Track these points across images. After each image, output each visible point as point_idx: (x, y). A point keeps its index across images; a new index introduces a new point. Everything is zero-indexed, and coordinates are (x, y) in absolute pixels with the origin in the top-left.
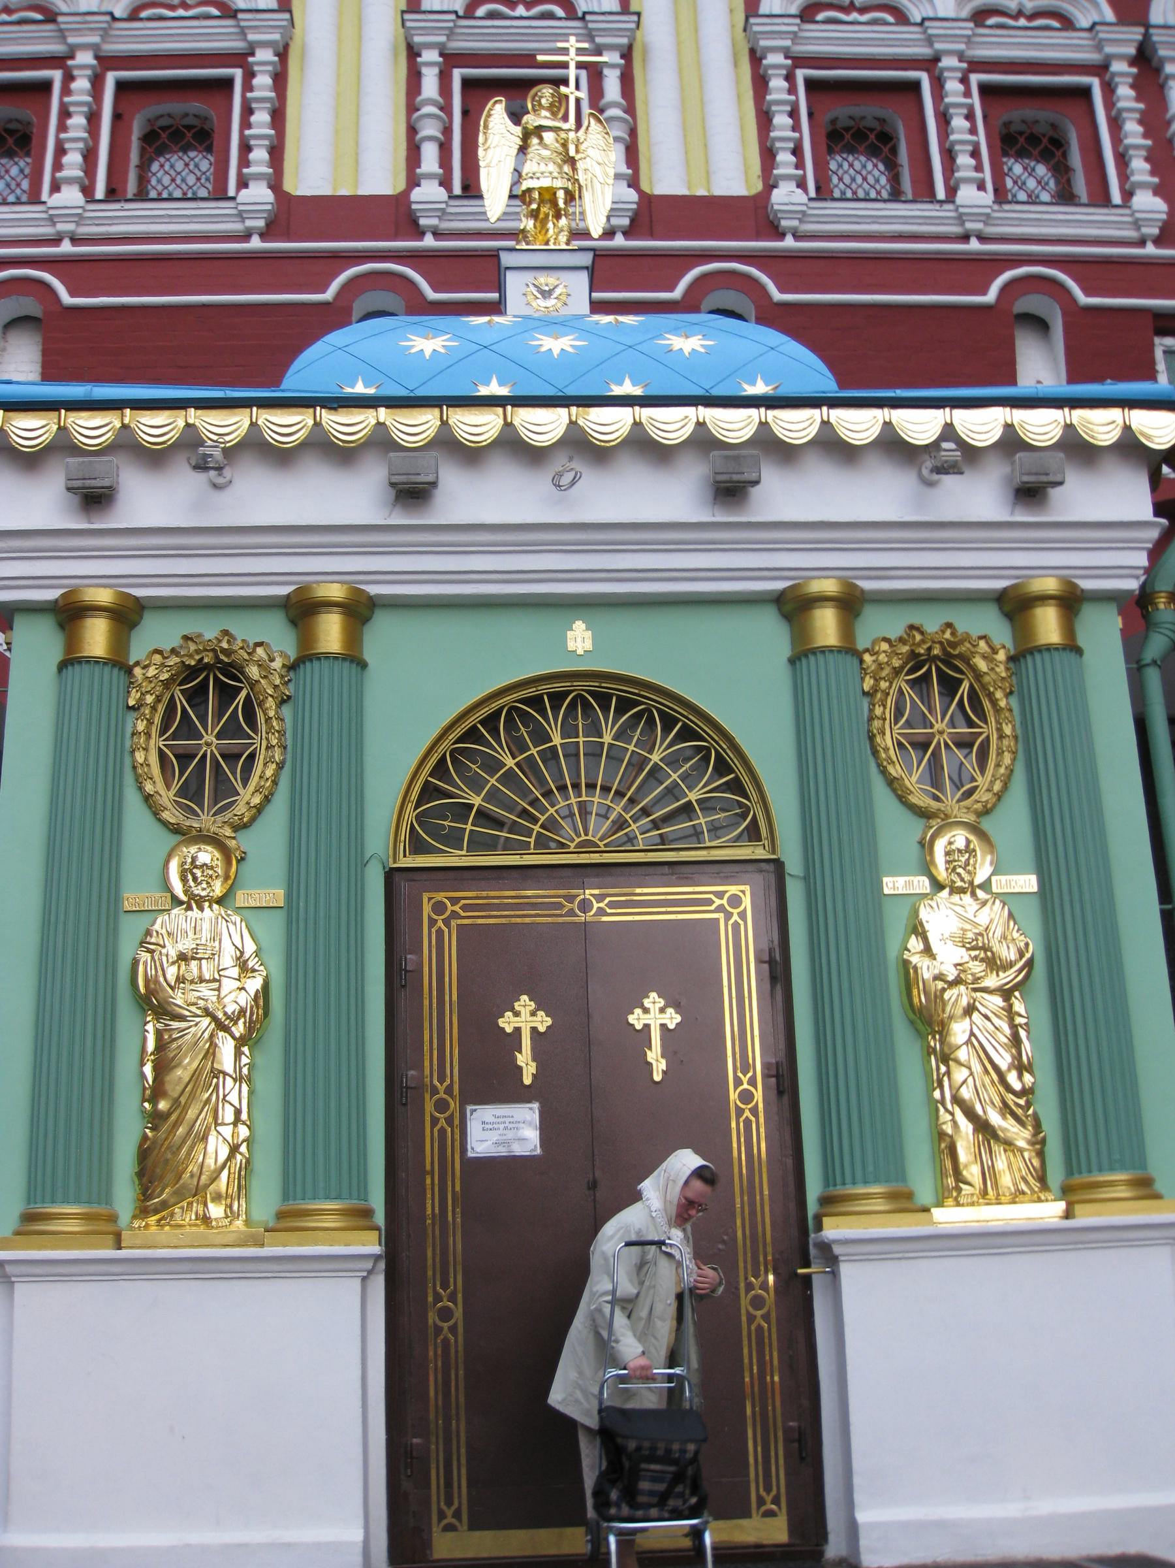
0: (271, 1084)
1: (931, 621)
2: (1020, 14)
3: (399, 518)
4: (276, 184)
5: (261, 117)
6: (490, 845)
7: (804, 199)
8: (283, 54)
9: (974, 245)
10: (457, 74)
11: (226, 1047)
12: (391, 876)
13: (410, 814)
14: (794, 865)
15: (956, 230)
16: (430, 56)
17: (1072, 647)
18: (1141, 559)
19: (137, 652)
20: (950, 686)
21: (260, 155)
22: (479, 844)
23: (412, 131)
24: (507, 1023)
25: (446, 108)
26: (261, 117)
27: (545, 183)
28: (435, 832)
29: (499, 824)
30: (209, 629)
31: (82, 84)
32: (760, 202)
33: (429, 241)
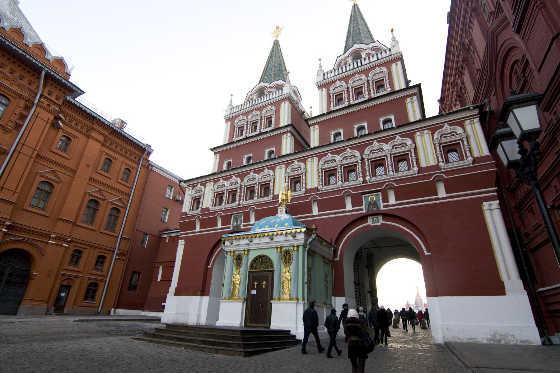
1: (287, 248)
2: (349, 156)
4: (273, 194)
6: (256, 269)
8: (274, 180)
9: (341, 188)
12: (249, 272)
13: (250, 267)
17: (298, 250)
18: (303, 242)
22: (255, 269)
29: (256, 267)
30: (239, 252)
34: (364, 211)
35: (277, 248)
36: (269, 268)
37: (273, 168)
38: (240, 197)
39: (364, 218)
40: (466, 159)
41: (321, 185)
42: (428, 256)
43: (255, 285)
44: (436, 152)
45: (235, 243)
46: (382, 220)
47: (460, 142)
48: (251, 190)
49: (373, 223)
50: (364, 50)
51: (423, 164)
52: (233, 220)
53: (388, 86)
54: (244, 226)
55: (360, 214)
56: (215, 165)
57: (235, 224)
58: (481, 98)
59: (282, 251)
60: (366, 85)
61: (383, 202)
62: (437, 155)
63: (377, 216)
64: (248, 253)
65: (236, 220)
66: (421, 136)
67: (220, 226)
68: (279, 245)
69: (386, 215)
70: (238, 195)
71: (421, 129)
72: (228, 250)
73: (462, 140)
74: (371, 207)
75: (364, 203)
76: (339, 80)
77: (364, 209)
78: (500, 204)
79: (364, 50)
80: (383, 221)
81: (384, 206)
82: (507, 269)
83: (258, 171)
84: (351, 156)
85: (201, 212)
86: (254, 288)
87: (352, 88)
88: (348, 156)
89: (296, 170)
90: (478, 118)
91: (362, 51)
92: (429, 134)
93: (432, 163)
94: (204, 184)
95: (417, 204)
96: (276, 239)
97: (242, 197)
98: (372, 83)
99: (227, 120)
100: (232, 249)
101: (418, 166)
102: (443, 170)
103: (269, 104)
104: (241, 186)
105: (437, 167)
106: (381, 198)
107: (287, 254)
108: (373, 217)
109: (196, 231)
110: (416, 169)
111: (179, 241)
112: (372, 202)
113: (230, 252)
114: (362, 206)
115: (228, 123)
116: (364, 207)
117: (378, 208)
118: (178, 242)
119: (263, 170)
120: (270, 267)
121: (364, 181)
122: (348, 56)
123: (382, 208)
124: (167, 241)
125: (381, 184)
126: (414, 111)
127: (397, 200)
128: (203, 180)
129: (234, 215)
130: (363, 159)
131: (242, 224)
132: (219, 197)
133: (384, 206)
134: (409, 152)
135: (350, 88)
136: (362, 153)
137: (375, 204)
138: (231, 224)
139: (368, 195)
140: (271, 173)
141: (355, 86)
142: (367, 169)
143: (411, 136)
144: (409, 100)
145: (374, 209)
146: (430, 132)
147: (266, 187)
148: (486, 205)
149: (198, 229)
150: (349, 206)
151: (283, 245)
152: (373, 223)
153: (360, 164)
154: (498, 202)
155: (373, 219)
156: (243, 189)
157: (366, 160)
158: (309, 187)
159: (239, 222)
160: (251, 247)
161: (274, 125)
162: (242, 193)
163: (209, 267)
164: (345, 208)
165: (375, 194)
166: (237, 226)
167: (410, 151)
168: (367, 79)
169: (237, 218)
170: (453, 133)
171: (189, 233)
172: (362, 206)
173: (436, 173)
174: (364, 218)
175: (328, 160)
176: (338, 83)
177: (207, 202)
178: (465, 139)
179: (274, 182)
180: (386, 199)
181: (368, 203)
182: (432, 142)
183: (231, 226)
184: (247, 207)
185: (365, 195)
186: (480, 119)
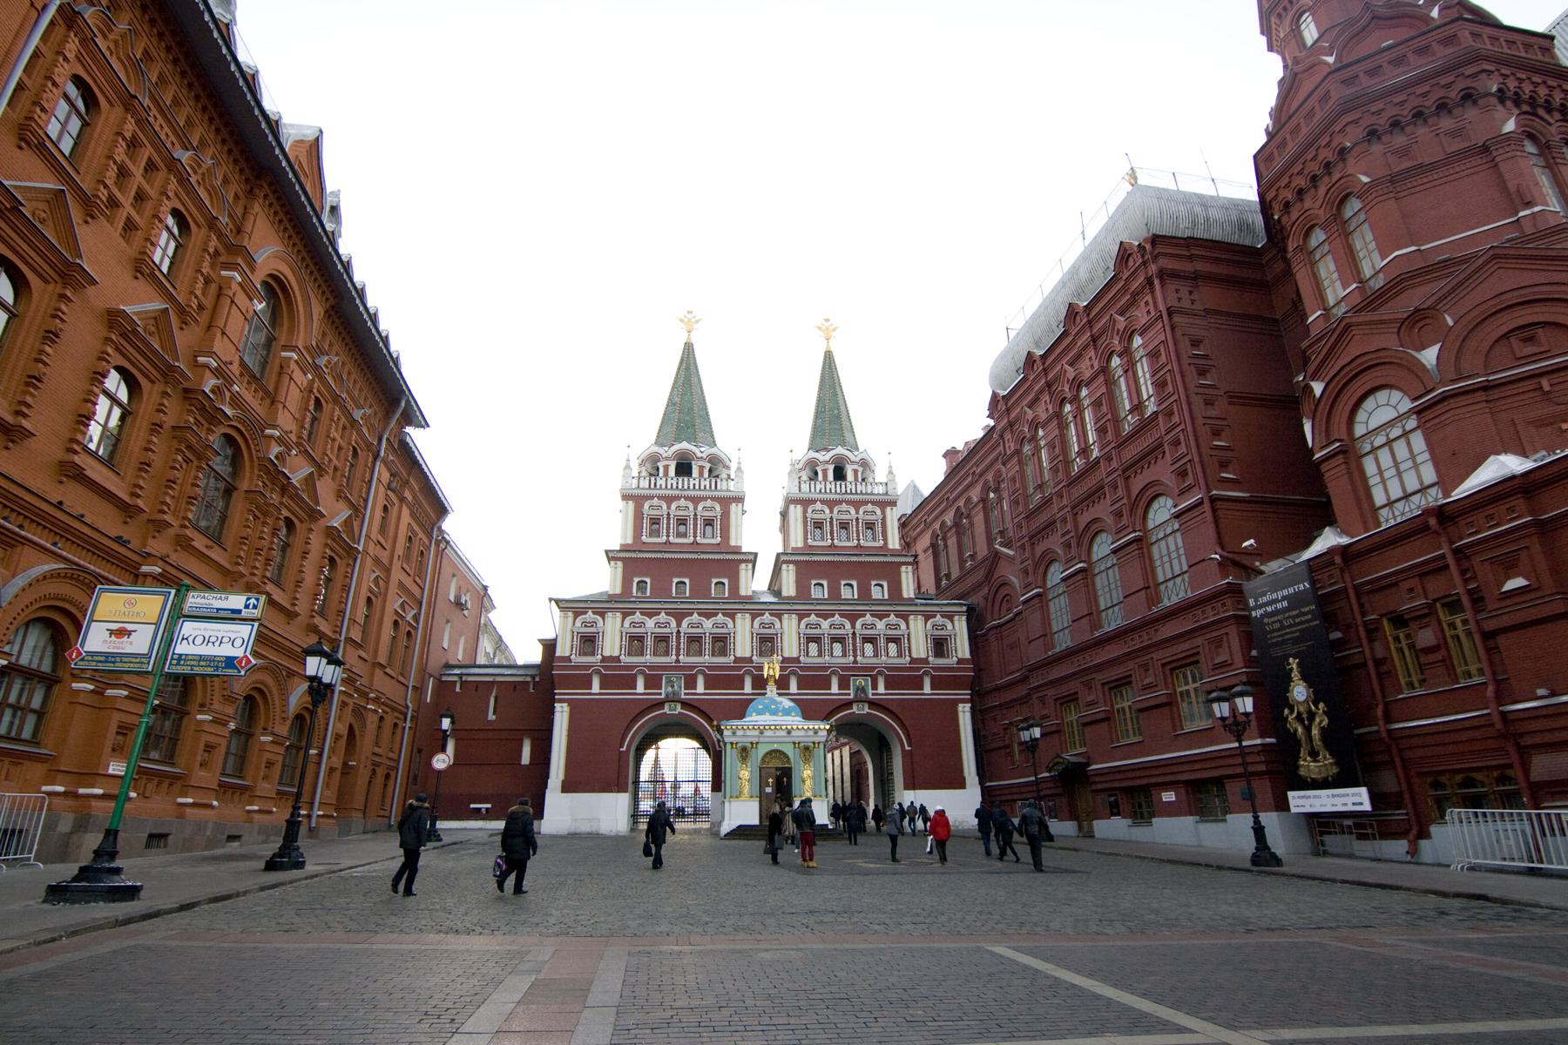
34: (852, 697)
35: (794, 743)
37: (732, 616)
38: (678, 649)
39: (849, 704)
45: (739, 733)
48: (695, 640)
51: (914, 655)
54: (685, 694)
57: (670, 689)
60: (854, 523)
65: (670, 682)
67: (640, 688)
68: (797, 740)
69: (873, 704)
71: (916, 613)
76: (823, 502)
77: (851, 694)
78: (971, 708)
81: (873, 694)
93: (923, 655)
94: (602, 614)
100: (734, 740)
104: (678, 632)
105: (925, 661)
109: (593, 691)
110: (908, 658)
113: (732, 743)
116: (851, 691)
117: (866, 694)
121: (855, 662)
123: (871, 696)
124: (458, 690)
126: (908, 584)
127: (886, 688)
128: (601, 606)
131: (683, 691)
132: (635, 642)
133: (873, 694)
136: (853, 626)
137: (862, 690)
144: (903, 568)
147: (722, 643)
148: (961, 706)
149: (596, 688)
150: (835, 688)
158: (786, 655)
160: (761, 740)
161: (719, 539)
170: (943, 627)
171: (578, 694)
173: (925, 668)
174: (849, 704)
176: (818, 506)
177: (612, 644)
180: (875, 687)
183: (663, 691)
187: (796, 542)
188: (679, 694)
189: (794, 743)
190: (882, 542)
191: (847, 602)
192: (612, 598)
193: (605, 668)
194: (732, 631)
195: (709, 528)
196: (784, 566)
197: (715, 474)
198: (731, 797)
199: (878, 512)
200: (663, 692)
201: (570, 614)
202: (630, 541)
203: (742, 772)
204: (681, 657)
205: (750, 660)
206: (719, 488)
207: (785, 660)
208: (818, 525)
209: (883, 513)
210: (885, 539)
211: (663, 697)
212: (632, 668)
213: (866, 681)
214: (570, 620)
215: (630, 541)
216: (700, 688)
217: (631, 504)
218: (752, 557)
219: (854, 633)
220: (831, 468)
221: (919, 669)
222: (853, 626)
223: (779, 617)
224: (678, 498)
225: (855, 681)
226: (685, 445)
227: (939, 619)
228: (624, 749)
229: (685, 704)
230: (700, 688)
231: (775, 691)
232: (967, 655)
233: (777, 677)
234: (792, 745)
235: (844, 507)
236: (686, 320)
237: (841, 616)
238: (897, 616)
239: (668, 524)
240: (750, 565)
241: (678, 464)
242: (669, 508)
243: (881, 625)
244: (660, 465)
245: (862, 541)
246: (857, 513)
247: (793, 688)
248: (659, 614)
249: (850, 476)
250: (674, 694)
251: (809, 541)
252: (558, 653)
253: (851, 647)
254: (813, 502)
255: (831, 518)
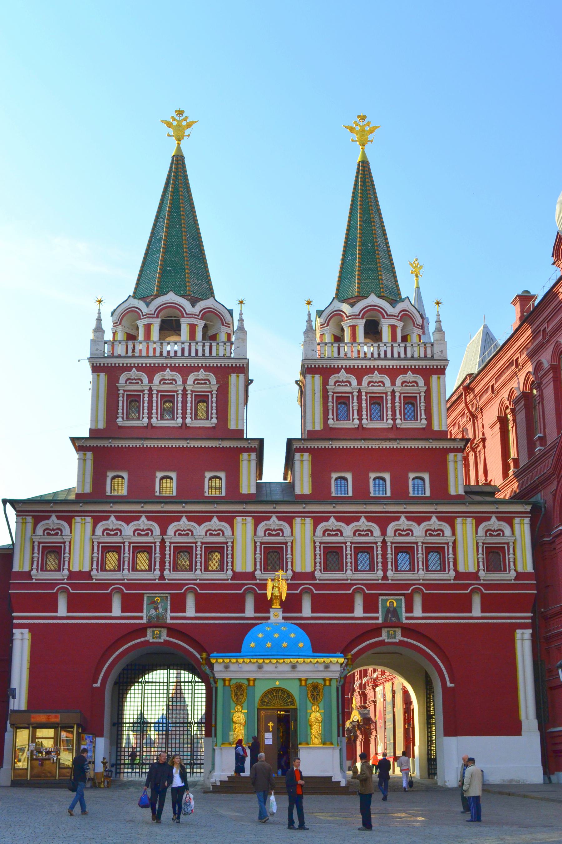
0: (246, 730)
1: (315, 681)
3: (259, 670)
4: (232, 570)
5: (230, 556)
7: (320, 574)
8: (233, 542)
9: (349, 582)
10: (263, 546)
11: (242, 726)
12: (258, 709)
14: (298, 709)
15: (346, 578)
16: (258, 544)
17: (330, 685)
18: (338, 675)
19: (231, 684)
20: (317, 688)
21: (230, 564)
22: (267, 705)
23: (255, 559)
24: (269, 725)
25: (261, 554)
26: (230, 556)
27: (277, 595)
28: (262, 704)
30: (239, 681)
31: (199, 549)
32: (313, 573)
33: (258, 581)
34: (380, 621)
35: (300, 680)
36: (288, 705)
40: (509, 573)
41: (318, 570)
42: (450, 688)
43: (270, 726)
44: (478, 555)
46: (400, 636)
47: (506, 546)
49: (388, 638)
50: (387, 315)
51: (461, 569)
52: (148, 605)
53: (423, 416)
54: (172, 618)
55: (373, 624)
56: (84, 474)
57: (153, 612)
58: (535, 481)
59: (307, 684)
60: (389, 398)
61: (406, 612)
62: (478, 559)
63: (394, 629)
64: (254, 683)
65: (152, 602)
66: (463, 524)
67: (117, 610)
68: (303, 676)
69: (407, 630)
70: (158, 559)
72: (220, 676)
73: (508, 544)
74: (390, 616)
75: (380, 610)
76: (349, 370)
78: (533, 635)
79: (387, 315)
80: (402, 636)
81: (407, 618)
82: (526, 707)
83: (200, 519)
84: (367, 530)
85: (69, 578)
86: (269, 731)
87: (367, 393)
88: (361, 529)
89: (274, 533)
90: (529, 518)
91: (384, 318)
92: (472, 524)
93: (472, 569)
95: (448, 621)
96: (300, 668)
97: (167, 564)
98: (400, 397)
99: (96, 369)
100: (227, 676)
101: (455, 570)
102: (482, 582)
103: (202, 367)
104: (163, 542)
105: (475, 576)
106: (403, 605)
107: (314, 689)
108: (389, 629)
109: (59, 614)
110: (452, 573)
111: (15, 631)
112: (391, 609)
113: (224, 680)
114: (378, 612)
115: (98, 376)
116: (380, 614)
117: (398, 618)
118: (12, 634)
119: (209, 519)
120: (291, 704)
121: (385, 577)
122: (359, 315)
123: (404, 621)
125: (406, 586)
127: (424, 611)
129: (148, 595)
130: (384, 542)
131: (169, 614)
133: (407, 618)
134: (446, 546)
135: (364, 394)
136: (384, 533)
137: (394, 612)
138: (145, 611)
139: (387, 597)
140: (226, 527)
141: (371, 391)
142: (389, 560)
143: (451, 522)
145: (393, 619)
146: (474, 521)
148: (519, 633)
149: (62, 610)
150: (359, 611)
151: (310, 676)
152: (388, 638)
153: (379, 549)
154: (530, 631)
155: (388, 632)
156: (168, 549)
157: (389, 544)
158: (298, 569)
159: (160, 610)
161: (214, 420)
162: (167, 556)
163: (95, 685)
164: (353, 612)
165: (396, 597)
166: (158, 617)
167: (447, 544)
168: (392, 388)
169: (155, 602)
172: (378, 612)
174: (376, 630)
175: (331, 529)
176: (343, 375)
178: (511, 544)
179: (232, 547)
180: (409, 609)
181: (386, 609)
182: (475, 538)
183: (144, 614)
184: (179, 586)
185: (382, 597)
186: (530, 520)
187: (314, 423)
188: (164, 618)
189: (300, 680)
190: (424, 422)
191: (377, 501)
192: (81, 498)
193: (74, 586)
194: (230, 540)
195: (202, 406)
196: (297, 456)
197: (211, 333)
198: (223, 744)
199: (421, 382)
200: (145, 615)
201: (30, 519)
202: (101, 425)
203: (237, 714)
204: (166, 573)
205: (251, 576)
206: (214, 354)
207: (296, 576)
208: (343, 400)
209: (427, 383)
210: (429, 418)
211: (144, 621)
212: (106, 586)
213: (399, 601)
214: (30, 526)
215: (101, 425)
216: (191, 611)
217: (103, 377)
218: (255, 445)
219: (384, 542)
220: (361, 324)
221: (466, 586)
222: (384, 533)
223: (289, 521)
224: (162, 368)
225: (384, 601)
226: (171, 297)
227: (494, 523)
228: (98, 685)
229: (172, 630)
230: (191, 611)
231: (280, 614)
232: (529, 568)
233: (284, 598)
234: (298, 683)
235: (376, 376)
236: (175, 123)
237: (368, 519)
238: (440, 519)
239: (150, 402)
240: (254, 455)
241: (163, 322)
242: (151, 381)
243: (419, 530)
244: (141, 324)
245: (398, 421)
246: (393, 384)
247: (307, 610)
248: (138, 518)
249: (386, 335)
250: (158, 617)
251: (330, 421)
252: (16, 568)
253: (380, 560)
254: (337, 370)
255: (359, 392)
